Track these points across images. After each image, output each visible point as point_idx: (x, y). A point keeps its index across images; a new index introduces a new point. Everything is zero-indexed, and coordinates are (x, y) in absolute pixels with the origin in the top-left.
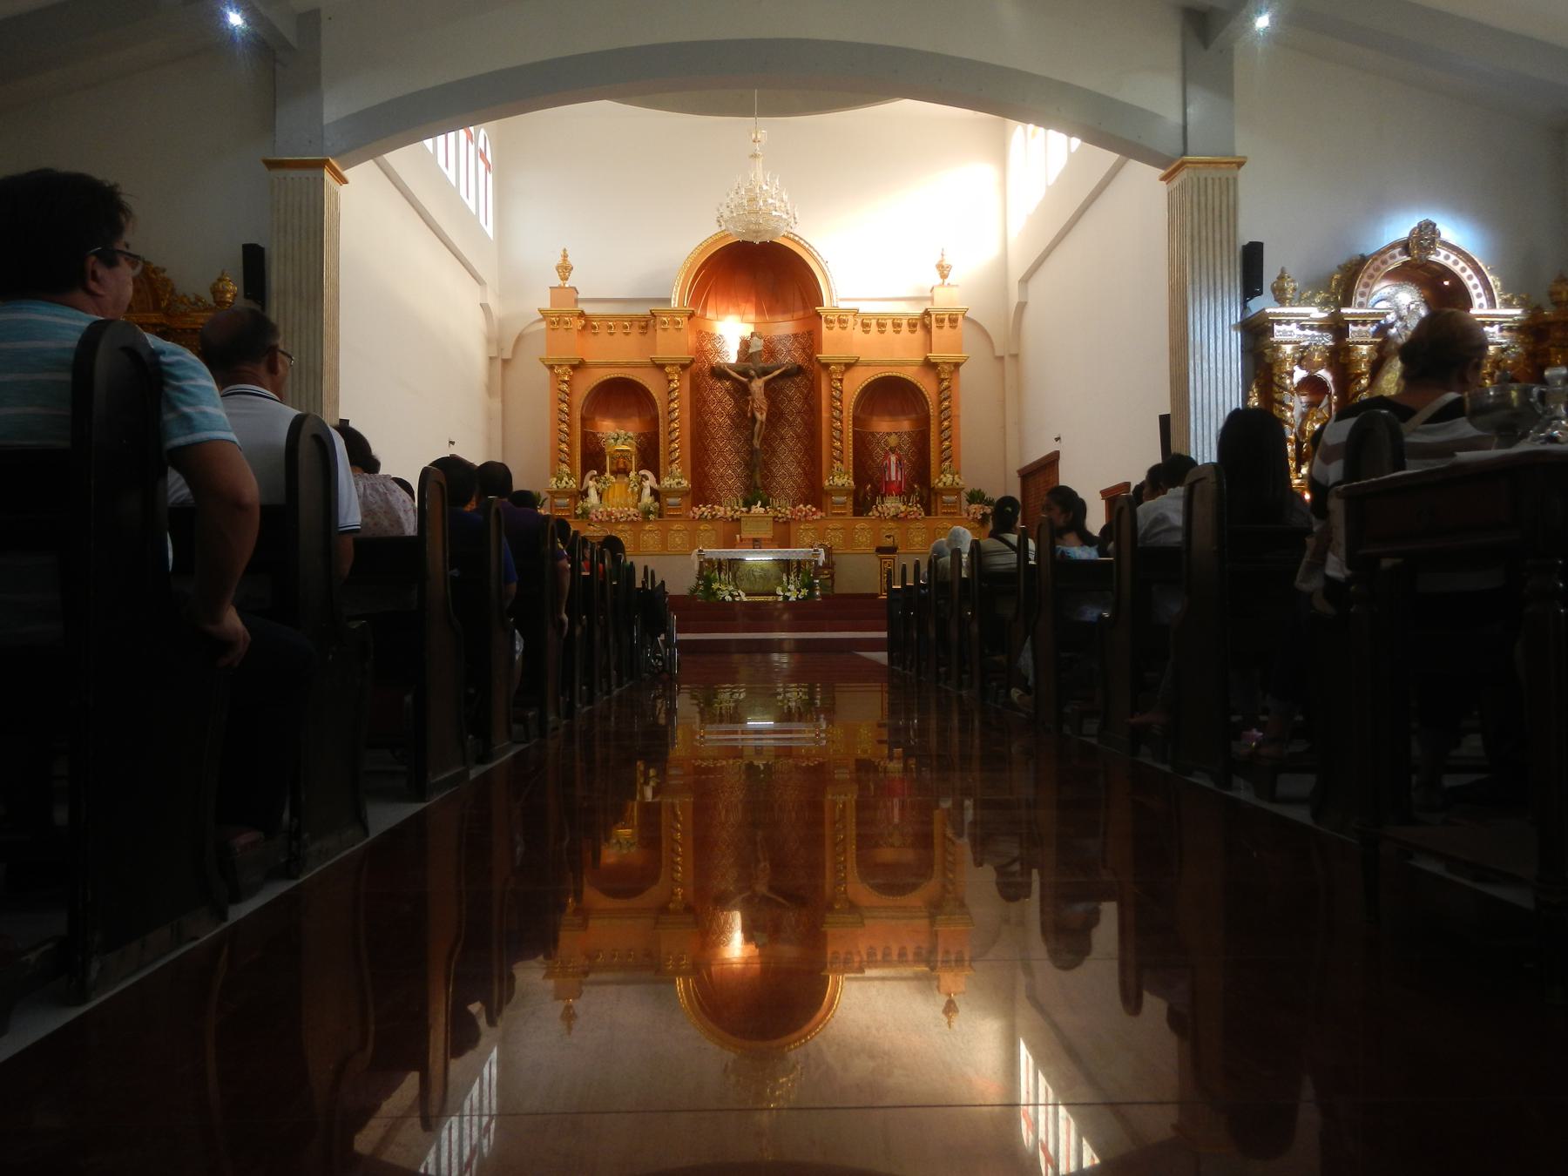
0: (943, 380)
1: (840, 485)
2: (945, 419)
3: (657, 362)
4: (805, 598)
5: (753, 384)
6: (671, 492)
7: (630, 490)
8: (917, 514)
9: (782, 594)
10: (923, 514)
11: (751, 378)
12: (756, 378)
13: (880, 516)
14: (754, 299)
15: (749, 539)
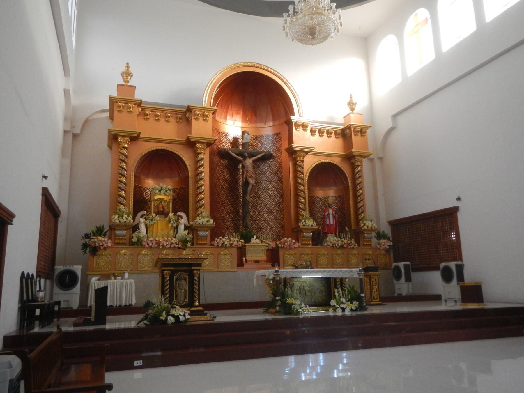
0: (358, 166)
1: (310, 225)
2: (360, 189)
3: (192, 140)
4: (356, 310)
5: (246, 161)
6: (203, 227)
7: (170, 225)
8: (353, 245)
9: (337, 306)
10: (357, 245)
11: (245, 158)
12: (248, 158)
13: (333, 246)
14: (242, 113)
15: (252, 261)
